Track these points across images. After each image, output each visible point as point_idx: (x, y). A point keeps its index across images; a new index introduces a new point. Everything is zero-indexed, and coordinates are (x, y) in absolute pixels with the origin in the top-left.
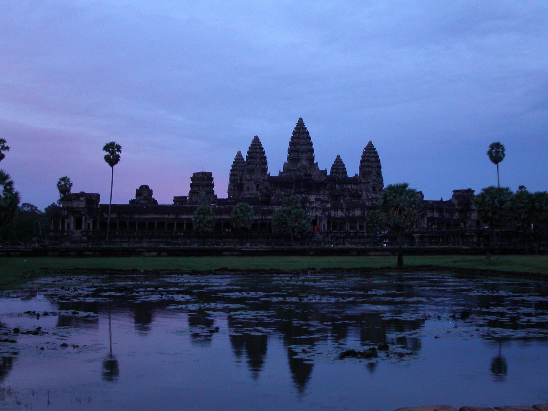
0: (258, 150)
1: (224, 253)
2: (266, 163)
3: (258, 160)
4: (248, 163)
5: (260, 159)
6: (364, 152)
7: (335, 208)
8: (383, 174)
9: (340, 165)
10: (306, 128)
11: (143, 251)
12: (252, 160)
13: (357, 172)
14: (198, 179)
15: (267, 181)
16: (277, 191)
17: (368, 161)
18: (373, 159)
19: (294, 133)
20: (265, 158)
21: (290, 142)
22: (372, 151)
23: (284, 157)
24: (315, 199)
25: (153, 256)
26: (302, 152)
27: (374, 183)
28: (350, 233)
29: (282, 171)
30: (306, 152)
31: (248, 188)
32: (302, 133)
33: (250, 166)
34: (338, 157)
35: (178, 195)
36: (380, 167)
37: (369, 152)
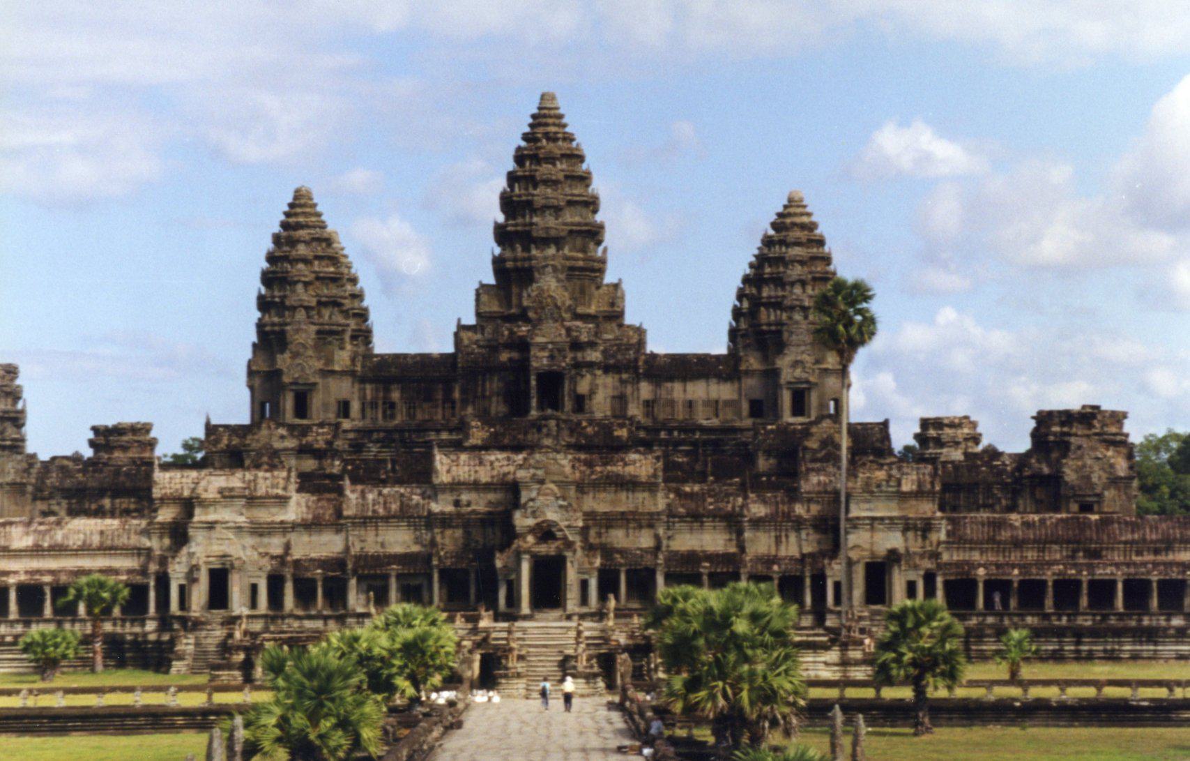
0: (302, 250)
3: (300, 288)
5: (306, 284)
6: (768, 242)
10: (569, 138)
17: (779, 281)
18: (796, 272)
19: (520, 158)
22: (796, 234)
23: (478, 261)
26: (545, 242)
27: (798, 372)
29: (470, 319)
30: (558, 242)
32: (551, 160)
35: (110, 422)
37: (783, 242)
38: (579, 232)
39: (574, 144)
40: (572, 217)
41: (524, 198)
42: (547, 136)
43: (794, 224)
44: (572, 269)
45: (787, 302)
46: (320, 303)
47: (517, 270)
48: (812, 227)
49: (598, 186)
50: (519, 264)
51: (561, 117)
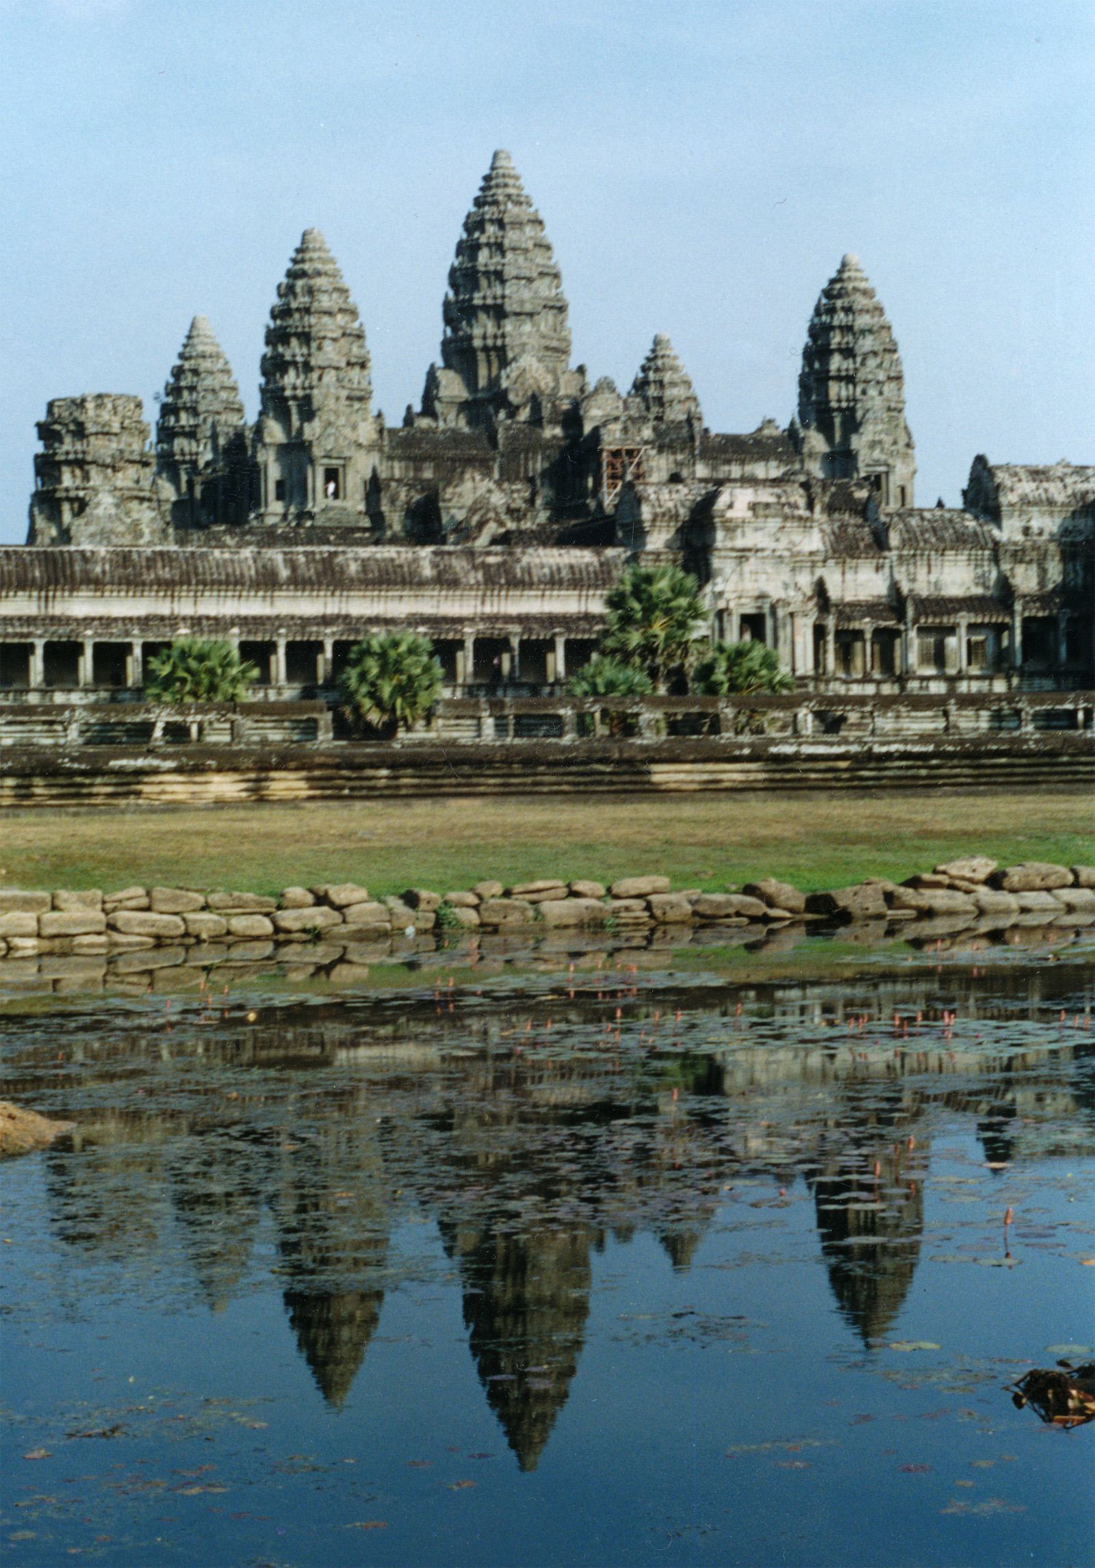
0: (325, 301)
1: (663, 774)
2: (363, 366)
3: (328, 346)
4: (273, 367)
7: (844, 549)
8: (912, 416)
9: (673, 384)
11: (155, 771)
12: (295, 349)
13: (783, 407)
14: (80, 432)
15: (371, 448)
16: (468, 485)
17: (848, 353)
19: (474, 225)
20: (360, 336)
21: (453, 272)
22: (860, 301)
24: (753, 507)
25: (221, 804)
27: (877, 454)
28: (928, 678)
29: (417, 408)
31: (280, 484)
33: (291, 378)
34: (657, 342)
36: (898, 378)
37: (848, 310)
38: (552, 307)
39: (532, 210)
40: (544, 288)
41: (492, 268)
42: (509, 196)
43: (855, 289)
44: (547, 348)
45: (861, 375)
46: (349, 364)
47: (486, 349)
48: (868, 293)
49: (561, 258)
50: (490, 342)
51: (517, 178)
